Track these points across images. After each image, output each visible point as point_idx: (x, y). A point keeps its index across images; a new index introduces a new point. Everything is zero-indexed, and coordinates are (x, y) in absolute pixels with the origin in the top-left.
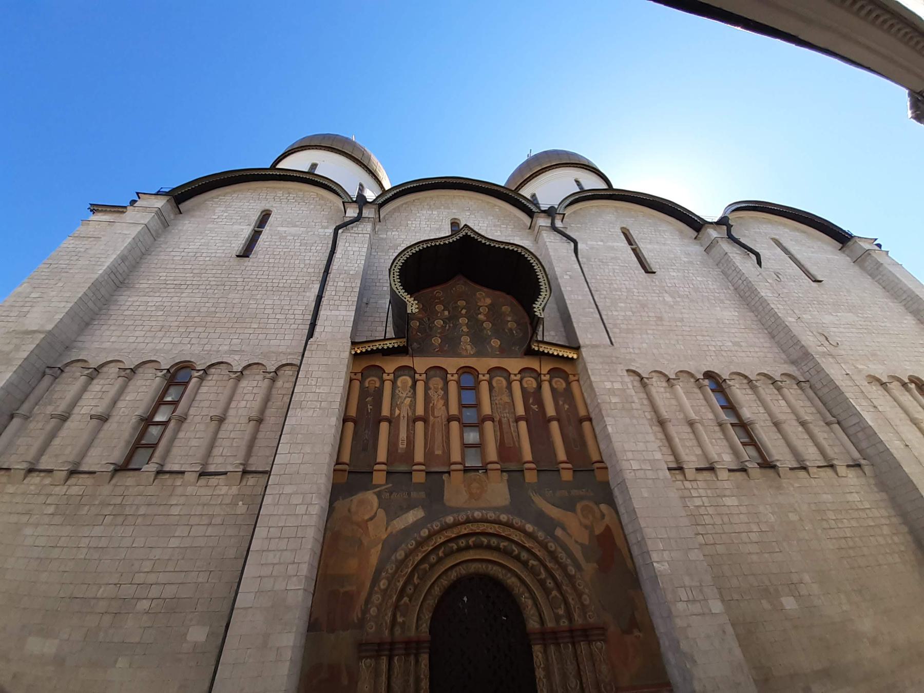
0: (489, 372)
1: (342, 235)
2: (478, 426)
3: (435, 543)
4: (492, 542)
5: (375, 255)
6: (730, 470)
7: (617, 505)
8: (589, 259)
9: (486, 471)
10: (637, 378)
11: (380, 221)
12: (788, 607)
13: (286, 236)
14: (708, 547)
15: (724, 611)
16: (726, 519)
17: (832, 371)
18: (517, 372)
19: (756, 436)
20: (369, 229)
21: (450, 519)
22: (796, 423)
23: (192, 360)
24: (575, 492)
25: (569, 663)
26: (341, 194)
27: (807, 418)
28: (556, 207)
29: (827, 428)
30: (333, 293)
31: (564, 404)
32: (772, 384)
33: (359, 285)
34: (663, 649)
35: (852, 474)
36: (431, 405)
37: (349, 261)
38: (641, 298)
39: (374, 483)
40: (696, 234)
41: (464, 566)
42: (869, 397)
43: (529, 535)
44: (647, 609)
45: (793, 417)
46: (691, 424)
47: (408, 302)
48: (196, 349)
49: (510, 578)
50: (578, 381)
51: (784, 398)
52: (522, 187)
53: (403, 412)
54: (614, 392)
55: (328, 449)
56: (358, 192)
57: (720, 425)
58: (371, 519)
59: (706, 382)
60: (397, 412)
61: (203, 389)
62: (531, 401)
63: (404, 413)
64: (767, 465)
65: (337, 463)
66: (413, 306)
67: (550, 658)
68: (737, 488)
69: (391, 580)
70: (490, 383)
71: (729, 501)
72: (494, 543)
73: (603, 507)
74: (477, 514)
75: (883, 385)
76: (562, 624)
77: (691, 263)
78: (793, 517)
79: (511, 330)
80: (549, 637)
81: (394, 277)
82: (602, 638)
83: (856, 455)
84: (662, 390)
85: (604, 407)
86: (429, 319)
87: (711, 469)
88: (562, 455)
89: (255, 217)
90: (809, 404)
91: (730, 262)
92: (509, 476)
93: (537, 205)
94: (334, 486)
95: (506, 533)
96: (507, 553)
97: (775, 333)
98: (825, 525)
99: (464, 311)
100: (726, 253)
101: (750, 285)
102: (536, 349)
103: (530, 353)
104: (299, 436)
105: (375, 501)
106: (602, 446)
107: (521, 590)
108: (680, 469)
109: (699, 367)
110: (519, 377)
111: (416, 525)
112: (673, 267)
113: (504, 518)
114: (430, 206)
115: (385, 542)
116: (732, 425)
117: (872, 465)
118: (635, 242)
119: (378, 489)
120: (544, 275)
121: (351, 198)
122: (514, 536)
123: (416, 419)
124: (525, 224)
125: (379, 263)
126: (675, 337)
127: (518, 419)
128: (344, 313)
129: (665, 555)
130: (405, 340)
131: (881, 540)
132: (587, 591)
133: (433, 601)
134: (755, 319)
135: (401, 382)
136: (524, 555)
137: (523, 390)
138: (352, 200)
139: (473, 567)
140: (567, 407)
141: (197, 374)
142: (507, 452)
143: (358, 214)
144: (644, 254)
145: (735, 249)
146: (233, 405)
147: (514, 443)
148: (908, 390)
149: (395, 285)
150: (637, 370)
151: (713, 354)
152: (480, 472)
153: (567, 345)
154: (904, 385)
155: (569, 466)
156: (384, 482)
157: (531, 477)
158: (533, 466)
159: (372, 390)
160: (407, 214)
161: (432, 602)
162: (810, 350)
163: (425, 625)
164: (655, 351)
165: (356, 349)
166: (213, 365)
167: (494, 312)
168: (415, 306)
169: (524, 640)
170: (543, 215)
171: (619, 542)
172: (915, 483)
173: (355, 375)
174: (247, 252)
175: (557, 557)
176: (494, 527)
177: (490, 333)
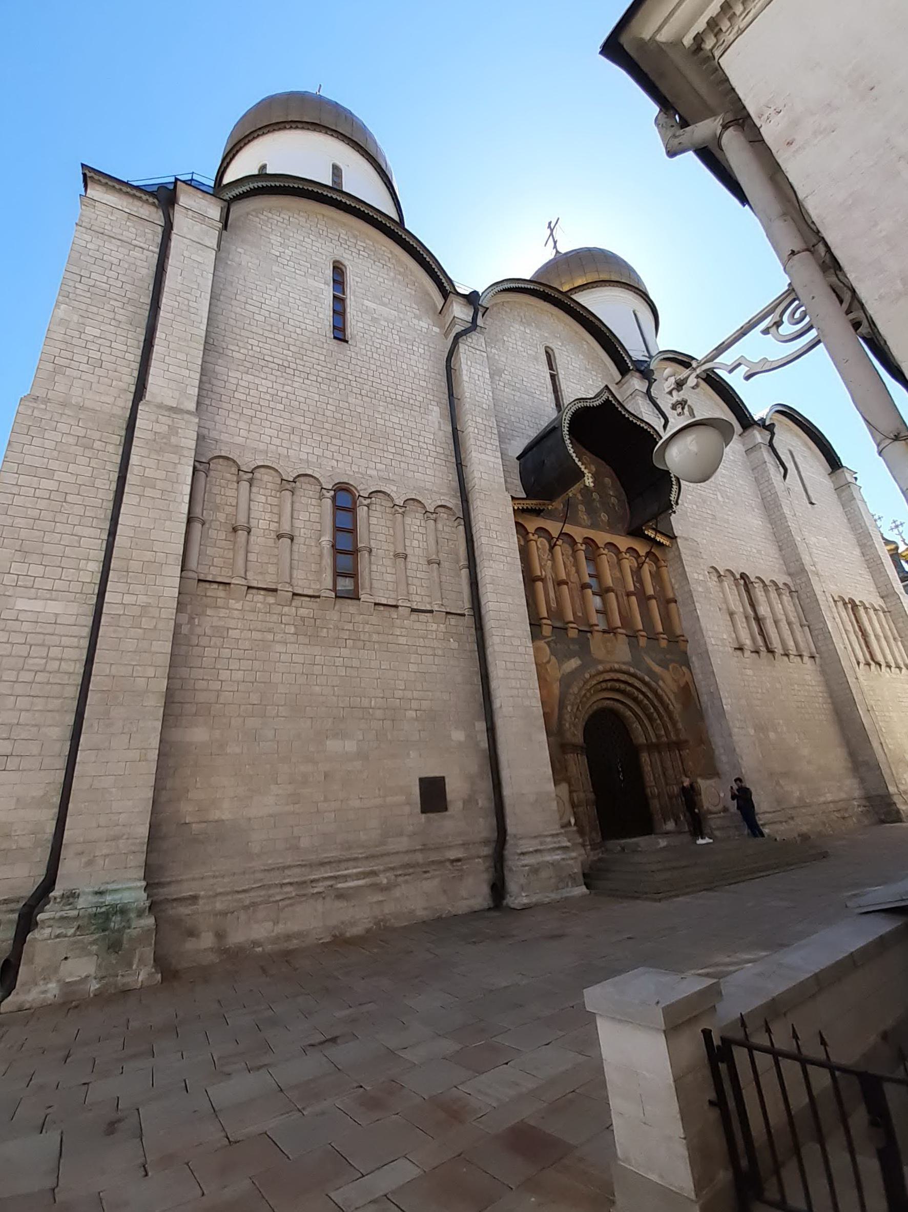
21: (600, 668)
23: (351, 483)
57: (746, 618)
64: (771, 651)
73: (683, 668)
74: (616, 666)
78: (778, 686)
80: (653, 747)
83: (814, 650)
97: (784, 547)
100: (765, 462)
127: (629, 594)
148: (846, 608)
154: (845, 604)
156: (549, 634)
157: (643, 642)
169: (633, 752)
170: (638, 374)
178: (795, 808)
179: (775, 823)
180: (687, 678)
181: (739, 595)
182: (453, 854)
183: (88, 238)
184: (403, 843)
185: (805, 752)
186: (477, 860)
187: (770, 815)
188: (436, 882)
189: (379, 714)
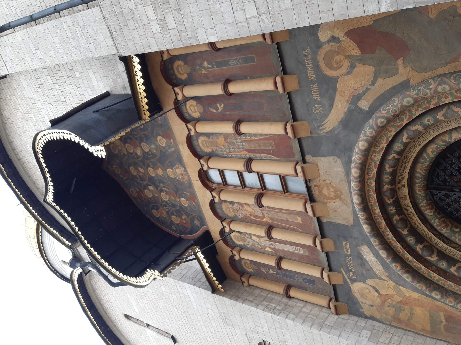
36: (252, 217)
39: (343, 283)
58: (377, 291)
60: (268, 249)
72: (388, 178)
74: (356, 199)
86: (165, 206)
92: (308, 154)
95: (374, 168)
107: (441, 143)
113: (355, 172)
115: (397, 284)
119: (348, 280)
122: (376, 159)
133: (457, 235)
136: (398, 146)
139: (419, 192)
140: (206, 64)
177: (153, 146)
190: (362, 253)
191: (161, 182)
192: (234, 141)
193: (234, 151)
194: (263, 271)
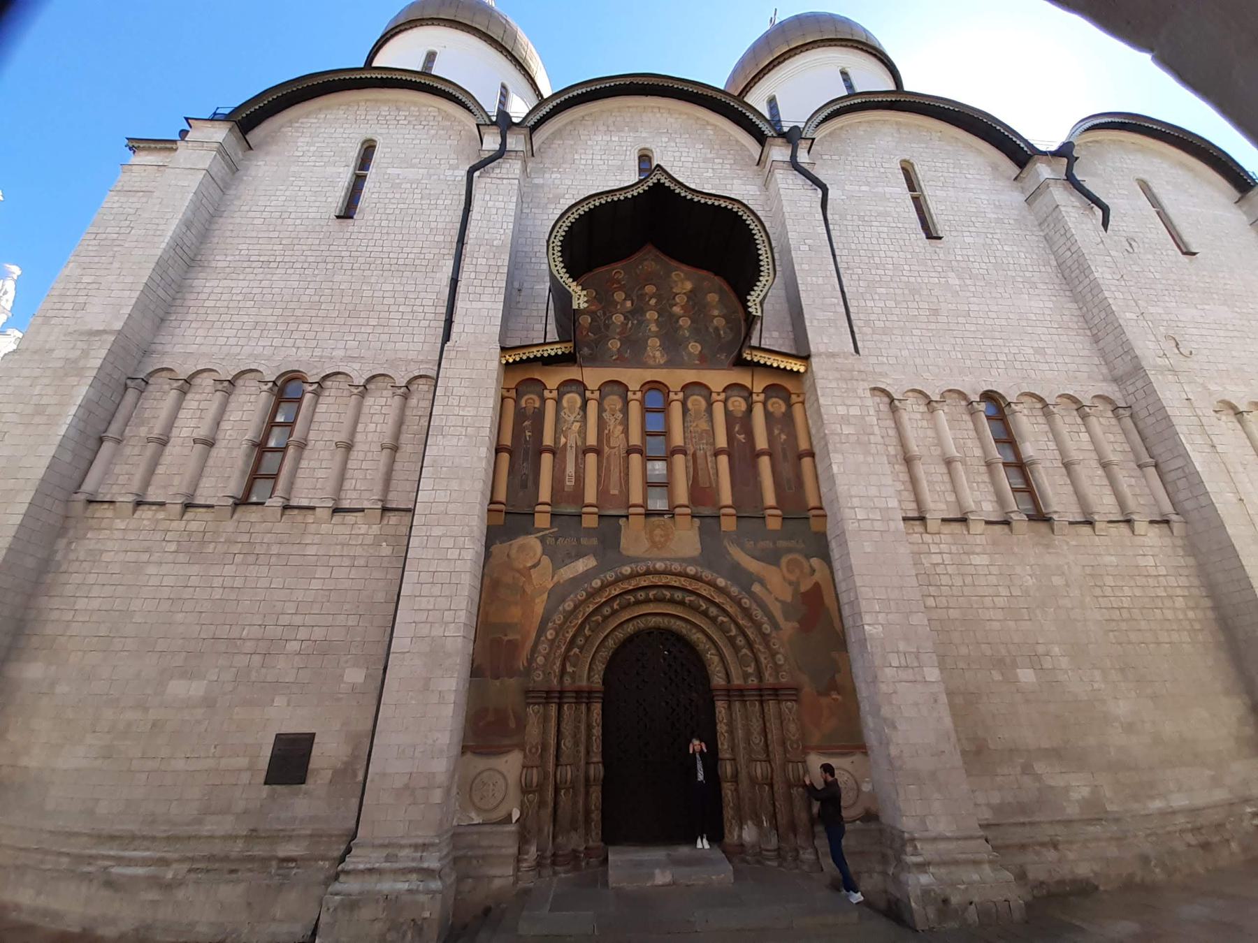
0: (684, 388)
1: (482, 184)
2: (668, 457)
3: (609, 594)
4: (676, 596)
5: (528, 214)
6: (988, 523)
7: (832, 559)
8: (843, 217)
9: (673, 517)
10: (886, 400)
11: (533, 155)
12: (1023, 680)
13: (402, 184)
14: (939, 610)
15: (940, 679)
16: (968, 580)
17: (1168, 394)
18: (721, 390)
19: (1034, 481)
20: (517, 171)
21: (627, 570)
22: (1094, 464)
23: (301, 370)
24: (782, 544)
25: (754, 720)
26: (474, 110)
27: (1113, 457)
28: (801, 125)
29: (1138, 472)
30: (473, 276)
31: (780, 434)
32: (1077, 410)
33: (506, 263)
34: (862, 714)
35: (1155, 531)
36: (606, 432)
37: (491, 224)
38: (912, 279)
40: (1016, 170)
41: (643, 619)
42: (1209, 433)
43: (722, 591)
44: (851, 672)
45: (1094, 455)
46: (949, 462)
47: (573, 293)
48: (304, 354)
49: (695, 634)
50: (803, 403)
51: (1088, 431)
52: (755, 83)
53: (571, 440)
54: (848, 420)
55: (479, 485)
56: (499, 108)
57: (989, 465)
58: (534, 566)
59: (983, 406)
60: (563, 440)
61: (321, 408)
62: (737, 429)
63: (571, 442)
64: (1040, 517)
65: (492, 502)
66: (580, 299)
67: (734, 715)
68: (993, 545)
69: (559, 630)
70: (684, 404)
71: (977, 560)
73: (815, 562)
74: (660, 566)
75: (1238, 416)
76: (750, 682)
77: (999, 221)
78: (1057, 581)
79: (717, 329)
80: (735, 694)
81: (553, 254)
82: (794, 698)
83: (1167, 507)
84: (919, 416)
85: (832, 440)
86: (605, 314)
87: (963, 520)
88: (770, 498)
89: (354, 153)
90: (1121, 438)
91: (1059, 220)
93: (775, 122)
94: (490, 529)
96: (693, 608)
98: (1098, 592)
99: (653, 302)
100: (1057, 206)
101: (1081, 260)
102: (749, 358)
103: (740, 363)
104: (444, 469)
105: (538, 548)
106: (823, 490)
108: (922, 519)
109: (974, 386)
110: (723, 396)
111: (587, 576)
112: (971, 229)
113: (691, 570)
114: (608, 127)
116: (1005, 465)
117: (1186, 522)
118: (920, 187)
119: (541, 534)
120: (767, 248)
121: (489, 117)
123: (587, 450)
124: (751, 156)
125: (535, 226)
126: (952, 340)
128: (490, 305)
129: (880, 618)
130: (571, 344)
131: (1169, 614)
132: (782, 650)
134: (1077, 313)
135: (568, 402)
136: (713, 611)
137: (728, 413)
138: (490, 120)
139: (653, 621)
140: (783, 437)
141: (310, 389)
142: (701, 493)
143: (500, 145)
144: (930, 206)
145: (1073, 199)
146: (360, 427)
147: (710, 483)
149: (556, 266)
150: (887, 389)
151: (1002, 365)
152: (666, 517)
153: (794, 352)
155: (778, 512)
156: (548, 526)
157: (728, 524)
158: (732, 511)
159: (530, 412)
160: (572, 143)
161: (605, 654)
162: (1144, 363)
163: (597, 676)
164: (918, 361)
165: (507, 357)
166: (328, 376)
167: (695, 301)
168: (583, 299)
169: (709, 696)
170: (780, 141)
171: (828, 600)
172: (1237, 548)
173: (508, 391)
174: (348, 212)
175: (751, 615)
176: (680, 580)
177: (687, 334)
178: (1068, 822)
179: (956, 863)
180: (820, 575)
181: (976, 430)
182: (286, 850)
183: (123, 199)
184: (226, 825)
185: (1122, 708)
186: (321, 863)
187: (952, 846)
188: (241, 888)
189: (249, 646)
190: (586, 557)
191: (640, 323)
192: (705, 441)
193: (692, 438)
194: (526, 423)
